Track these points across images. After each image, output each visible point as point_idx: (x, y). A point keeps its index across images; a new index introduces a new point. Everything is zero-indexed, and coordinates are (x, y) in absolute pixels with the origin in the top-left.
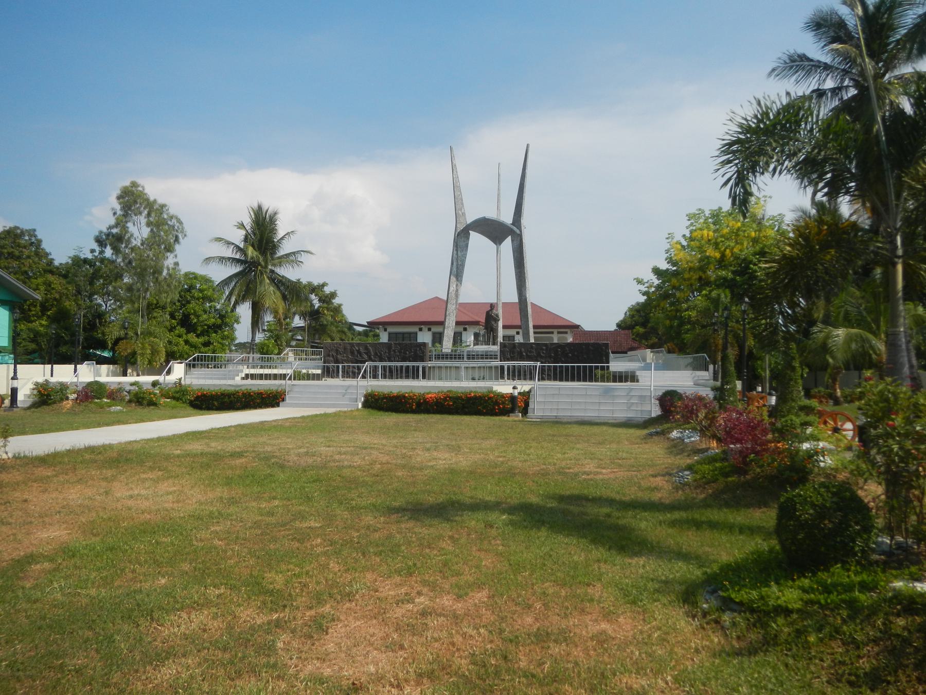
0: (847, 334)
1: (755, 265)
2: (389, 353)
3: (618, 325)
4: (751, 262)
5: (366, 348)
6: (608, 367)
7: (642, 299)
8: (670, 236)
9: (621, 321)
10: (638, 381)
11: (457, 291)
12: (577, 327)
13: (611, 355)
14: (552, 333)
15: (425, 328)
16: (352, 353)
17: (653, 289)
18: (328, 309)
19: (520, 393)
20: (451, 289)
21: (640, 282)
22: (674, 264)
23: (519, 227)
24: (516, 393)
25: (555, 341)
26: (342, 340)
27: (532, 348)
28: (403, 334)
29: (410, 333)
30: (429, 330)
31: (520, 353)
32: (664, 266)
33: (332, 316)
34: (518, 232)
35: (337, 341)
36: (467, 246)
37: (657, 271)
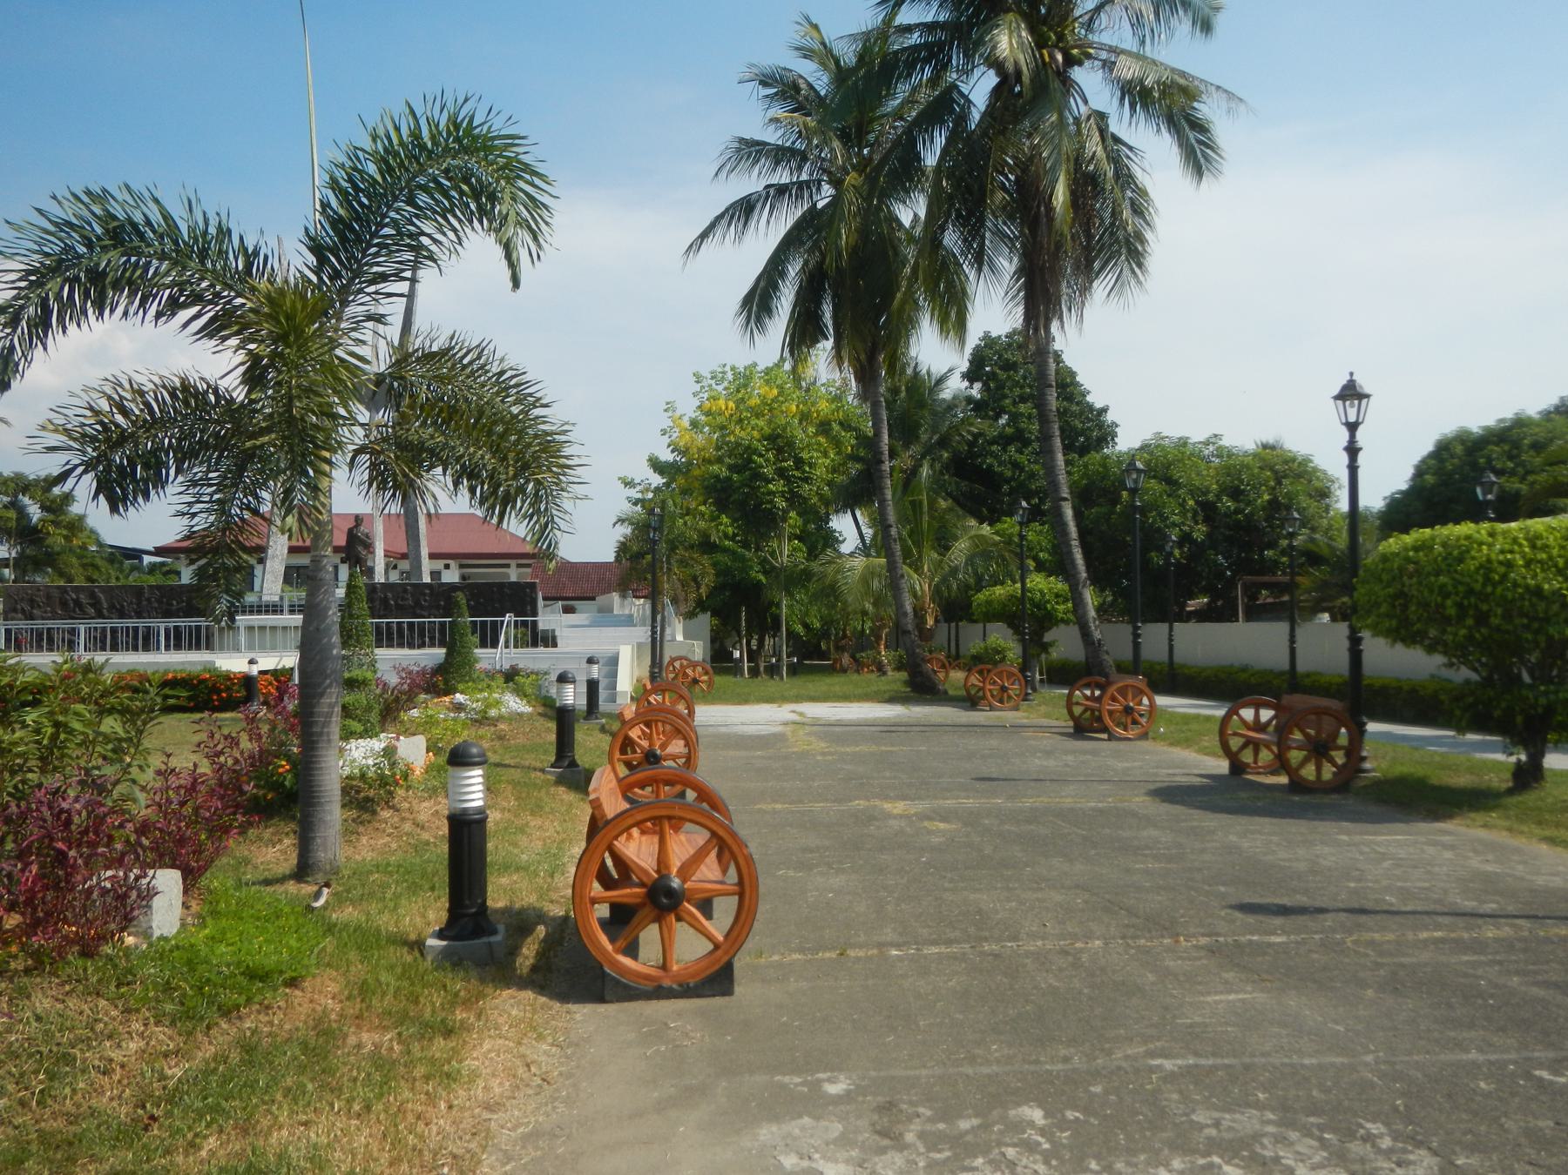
0: (867, 567)
1: (761, 456)
2: (139, 604)
4: (756, 452)
5: (92, 595)
6: (535, 623)
8: (669, 407)
10: (555, 645)
13: (541, 603)
14: (508, 566)
16: (64, 604)
17: (650, 495)
18: (56, 524)
19: (261, 672)
21: (629, 484)
24: (255, 670)
25: (513, 578)
26: (90, 579)
27: (405, 591)
31: (385, 601)
32: (667, 456)
33: (66, 537)
35: (80, 582)
37: (657, 466)
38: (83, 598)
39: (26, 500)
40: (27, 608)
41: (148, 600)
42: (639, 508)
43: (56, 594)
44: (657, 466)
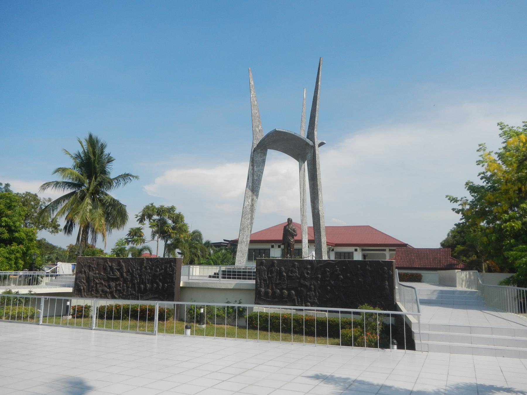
2: (141, 270)
3: (442, 244)
5: (119, 264)
7: (458, 218)
8: (481, 148)
9: (445, 241)
11: (252, 205)
12: (405, 245)
14: (385, 250)
15: (276, 246)
16: (105, 269)
17: (468, 207)
20: (247, 203)
22: (488, 179)
23: (313, 140)
27: (294, 266)
28: (260, 250)
29: (265, 250)
30: (279, 247)
31: (280, 273)
32: (480, 182)
34: (311, 143)
36: (264, 161)
37: (472, 189)
38: (115, 266)
39: (166, 218)
40: (87, 271)
41: (146, 267)
42: (460, 215)
43: (101, 262)
44: (472, 189)
